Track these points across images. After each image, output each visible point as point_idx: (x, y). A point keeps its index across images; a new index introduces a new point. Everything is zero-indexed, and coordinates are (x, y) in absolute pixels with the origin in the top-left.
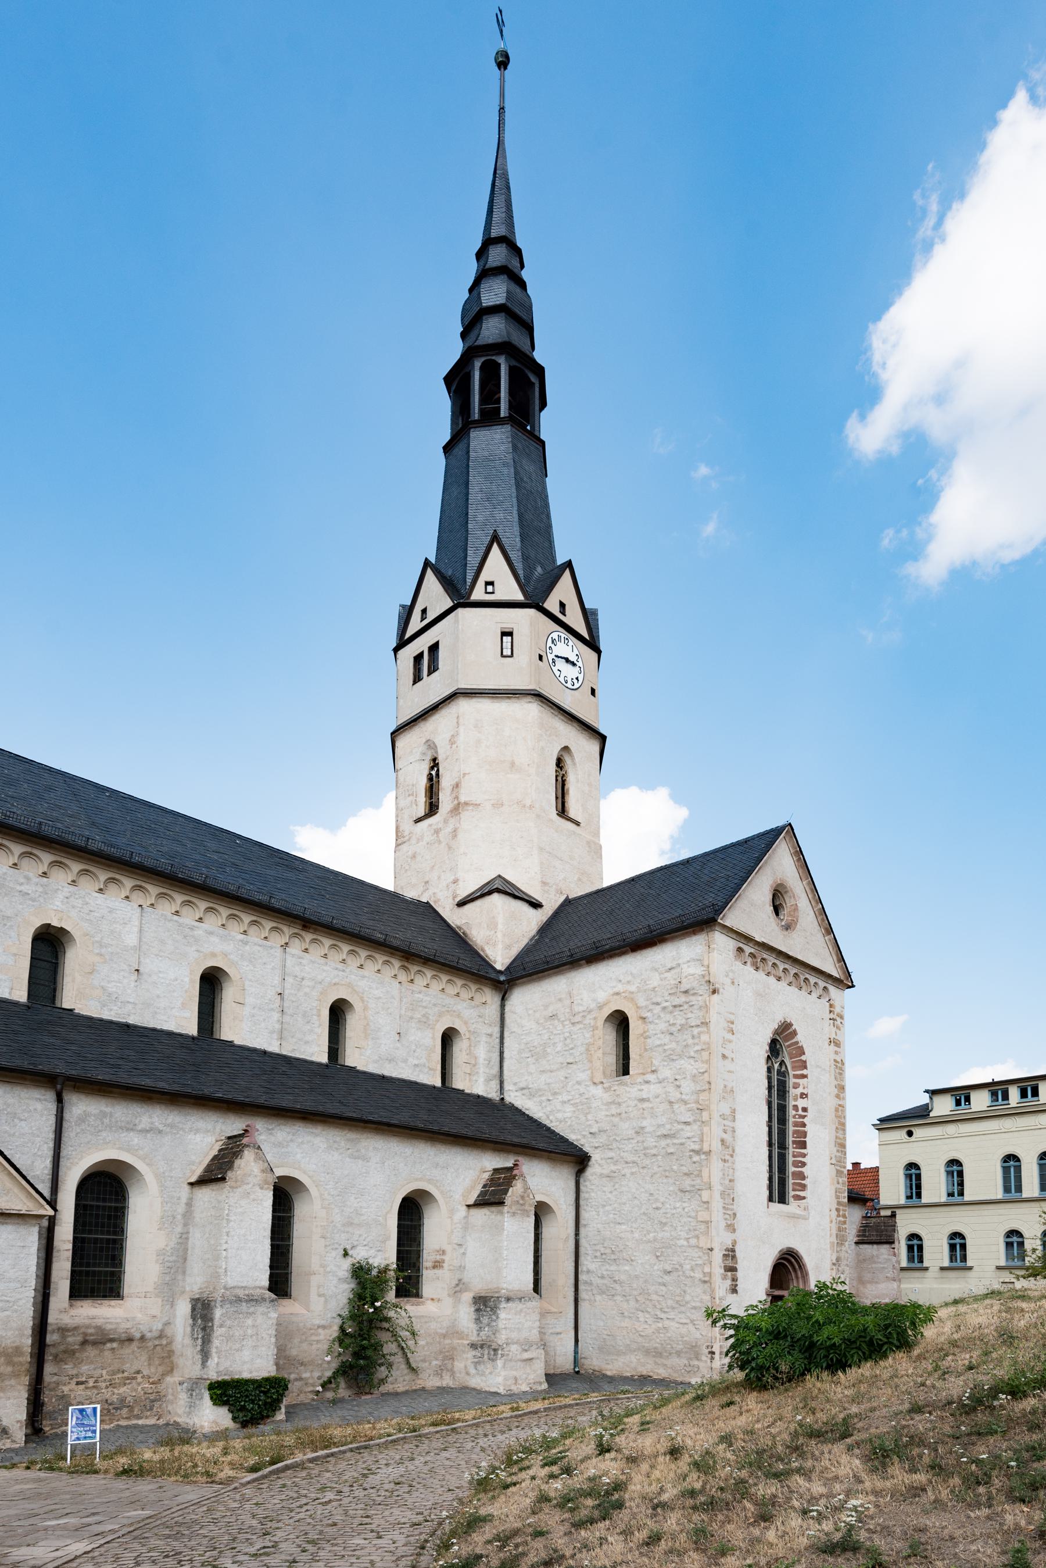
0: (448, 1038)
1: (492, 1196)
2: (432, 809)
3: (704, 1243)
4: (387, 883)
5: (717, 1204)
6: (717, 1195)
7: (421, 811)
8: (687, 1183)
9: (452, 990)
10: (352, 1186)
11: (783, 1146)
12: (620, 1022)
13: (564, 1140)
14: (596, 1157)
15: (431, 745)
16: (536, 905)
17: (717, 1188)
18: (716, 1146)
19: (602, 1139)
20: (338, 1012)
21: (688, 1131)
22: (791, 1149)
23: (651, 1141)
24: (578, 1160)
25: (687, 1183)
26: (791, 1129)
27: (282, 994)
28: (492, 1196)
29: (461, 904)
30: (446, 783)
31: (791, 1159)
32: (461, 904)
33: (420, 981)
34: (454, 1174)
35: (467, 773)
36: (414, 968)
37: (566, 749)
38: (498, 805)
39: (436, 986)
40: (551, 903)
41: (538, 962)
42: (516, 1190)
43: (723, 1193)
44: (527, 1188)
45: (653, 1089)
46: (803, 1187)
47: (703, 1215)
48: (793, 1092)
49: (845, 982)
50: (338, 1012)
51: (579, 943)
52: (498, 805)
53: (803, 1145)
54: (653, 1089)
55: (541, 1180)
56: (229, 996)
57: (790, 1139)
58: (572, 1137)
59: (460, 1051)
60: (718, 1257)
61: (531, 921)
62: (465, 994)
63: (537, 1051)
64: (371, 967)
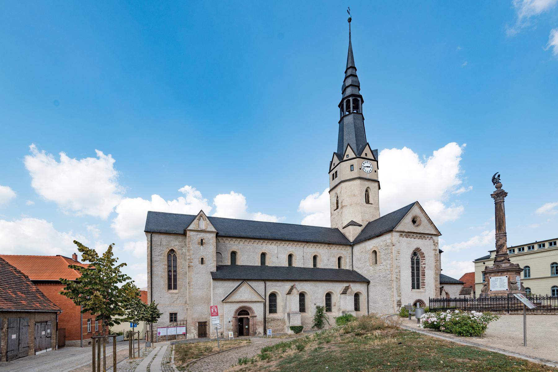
0: (339, 259)
1: (344, 292)
2: (337, 207)
3: (392, 299)
4: (329, 226)
5: (395, 291)
6: (395, 289)
7: (335, 208)
8: (389, 287)
9: (340, 249)
10: (316, 293)
11: (418, 275)
12: (375, 252)
13: (365, 278)
14: (371, 281)
15: (336, 194)
16: (360, 226)
17: (395, 288)
18: (394, 279)
19: (372, 278)
20: (315, 258)
21: (389, 276)
22: (421, 276)
23: (382, 278)
24: (368, 282)
25: (389, 287)
26: (421, 272)
27: (303, 256)
28: (344, 292)
29: (344, 228)
30: (340, 202)
31: (421, 279)
32: (344, 228)
33: (332, 248)
34: (337, 288)
35: (345, 200)
36: (331, 246)
37: (368, 187)
38: (351, 205)
39: (336, 248)
40: (364, 224)
41: (359, 240)
42: (349, 290)
43: (397, 289)
44: (352, 290)
45: (382, 267)
46: (424, 285)
47: (392, 294)
48: (421, 263)
49: (439, 234)
50: (315, 258)
51: (367, 236)
52: (351, 205)
53: (424, 275)
54: (382, 267)
55: (356, 288)
56: (294, 258)
57: (421, 274)
58: (367, 277)
59: (342, 261)
60: (395, 303)
61: (359, 230)
62: (343, 249)
63: (359, 259)
64: (321, 247)
